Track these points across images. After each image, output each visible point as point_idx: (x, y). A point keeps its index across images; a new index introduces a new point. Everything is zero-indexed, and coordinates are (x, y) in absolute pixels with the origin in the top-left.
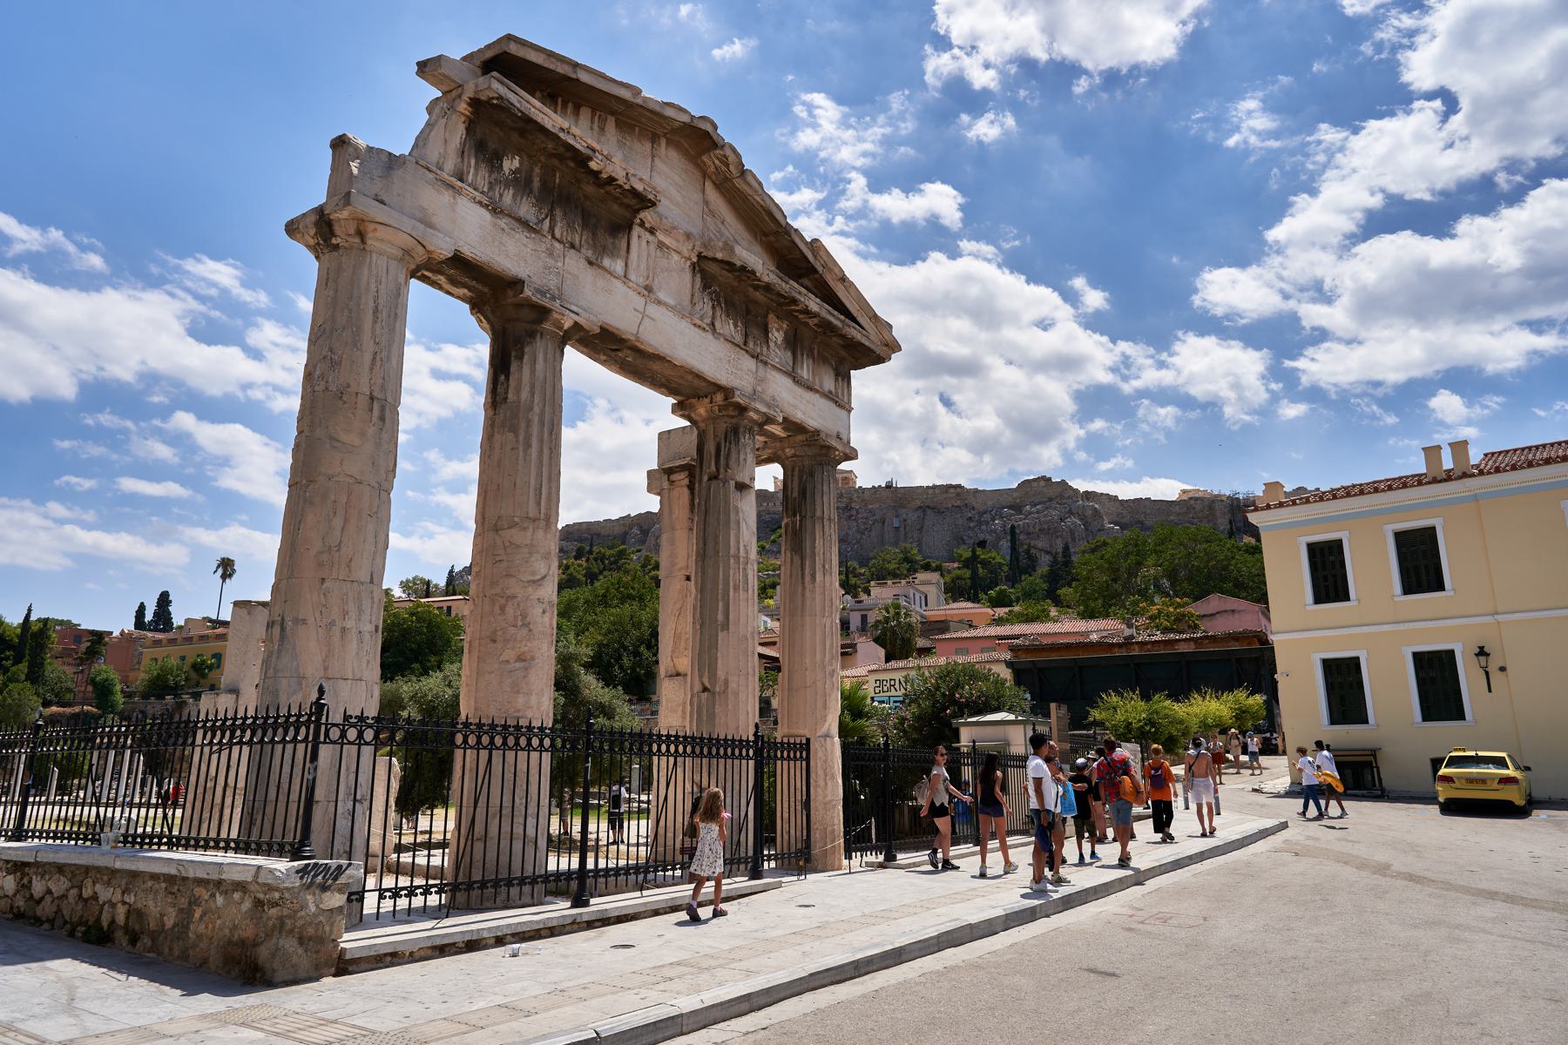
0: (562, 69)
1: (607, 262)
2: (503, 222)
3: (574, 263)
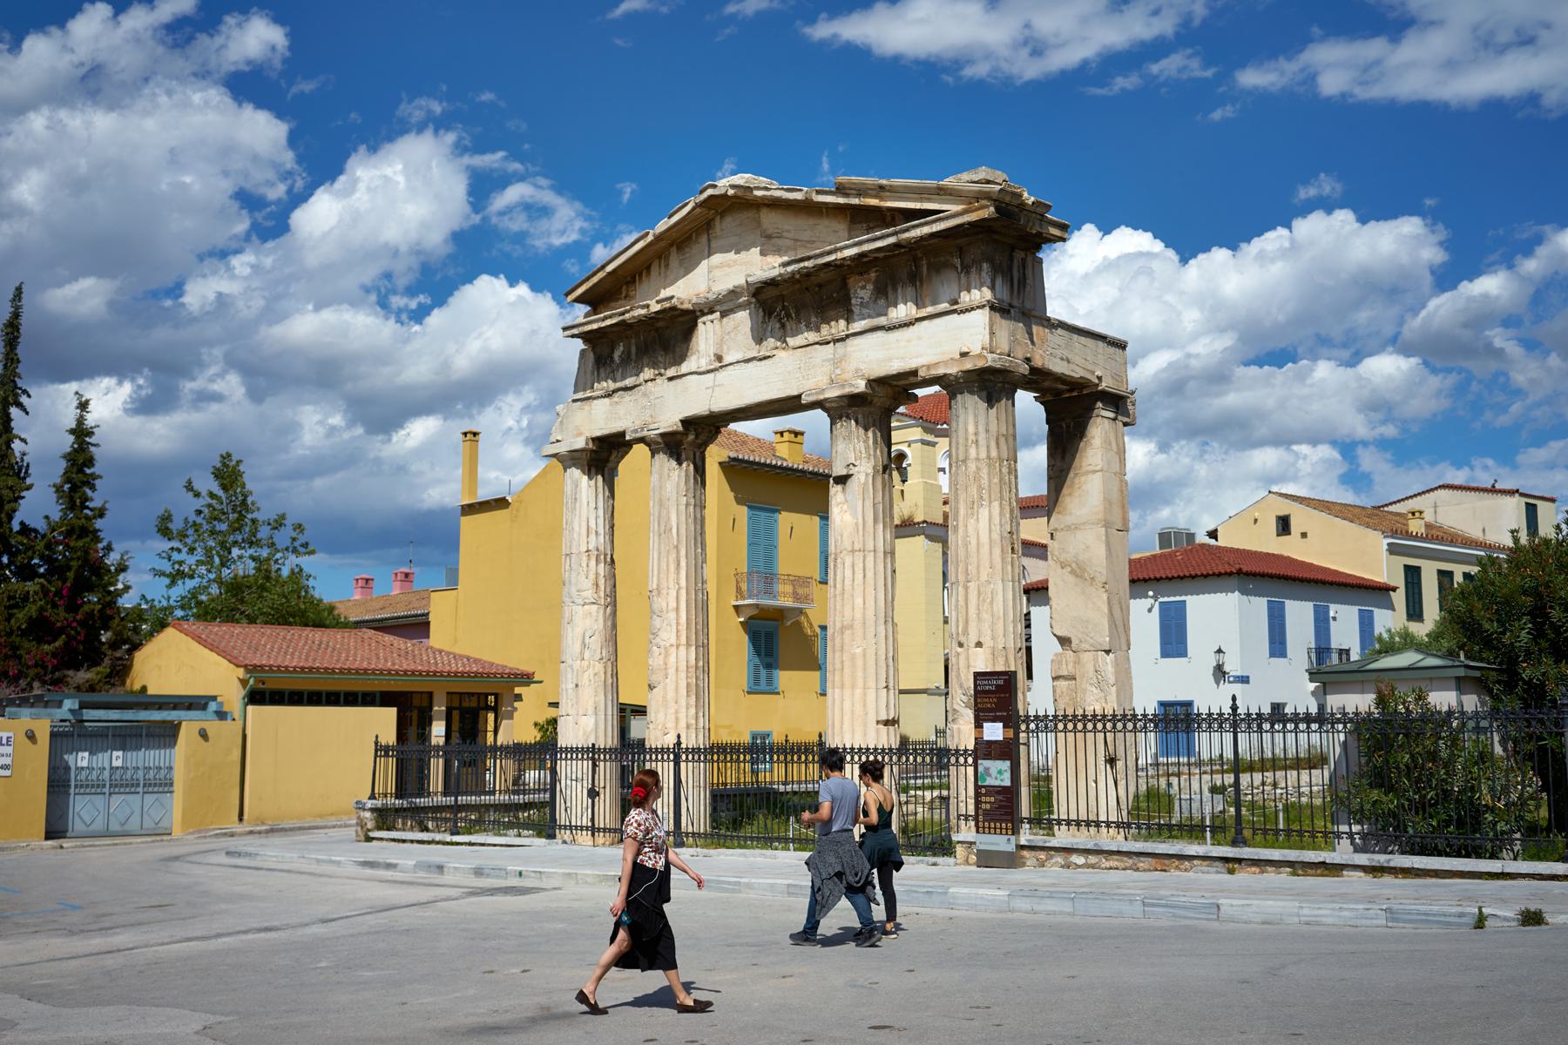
0: (601, 275)
1: (685, 367)
2: (616, 398)
3: (661, 388)
